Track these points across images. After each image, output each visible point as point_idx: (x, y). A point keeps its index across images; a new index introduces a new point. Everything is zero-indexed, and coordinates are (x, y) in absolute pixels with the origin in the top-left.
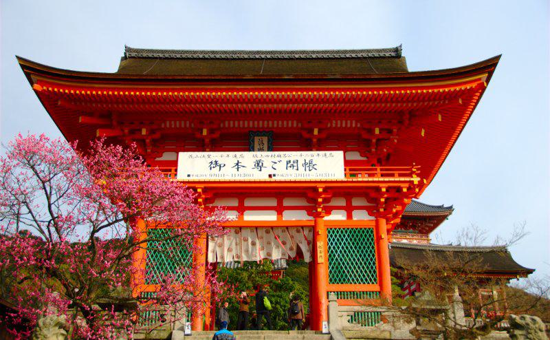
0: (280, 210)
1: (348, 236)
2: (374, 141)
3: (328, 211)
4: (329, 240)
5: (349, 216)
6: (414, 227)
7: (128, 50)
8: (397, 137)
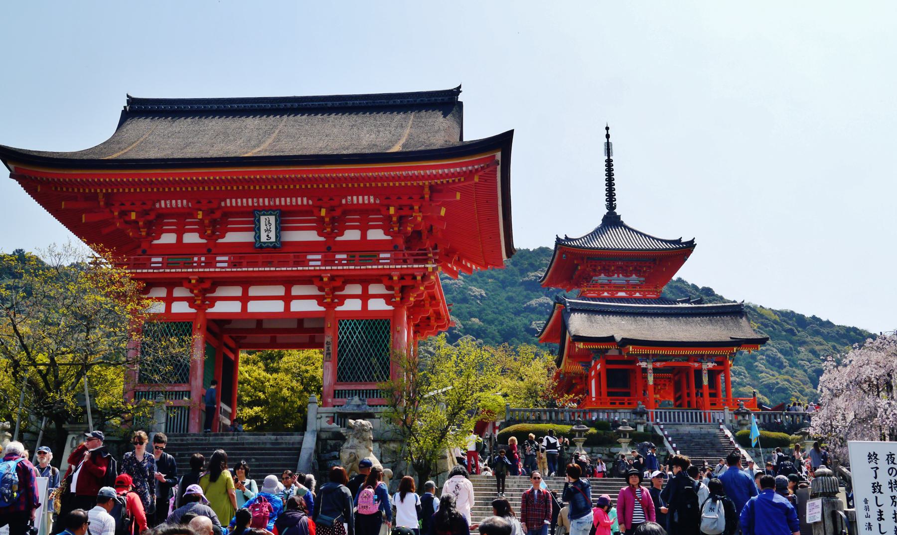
0: (287, 299)
1: (362, 328)
2: (394, 219)
3: (342, 299)
4: (341, 333)
5: (365, 305)
6: (638, 272)
7: (132, 101)
8: (421, 214)
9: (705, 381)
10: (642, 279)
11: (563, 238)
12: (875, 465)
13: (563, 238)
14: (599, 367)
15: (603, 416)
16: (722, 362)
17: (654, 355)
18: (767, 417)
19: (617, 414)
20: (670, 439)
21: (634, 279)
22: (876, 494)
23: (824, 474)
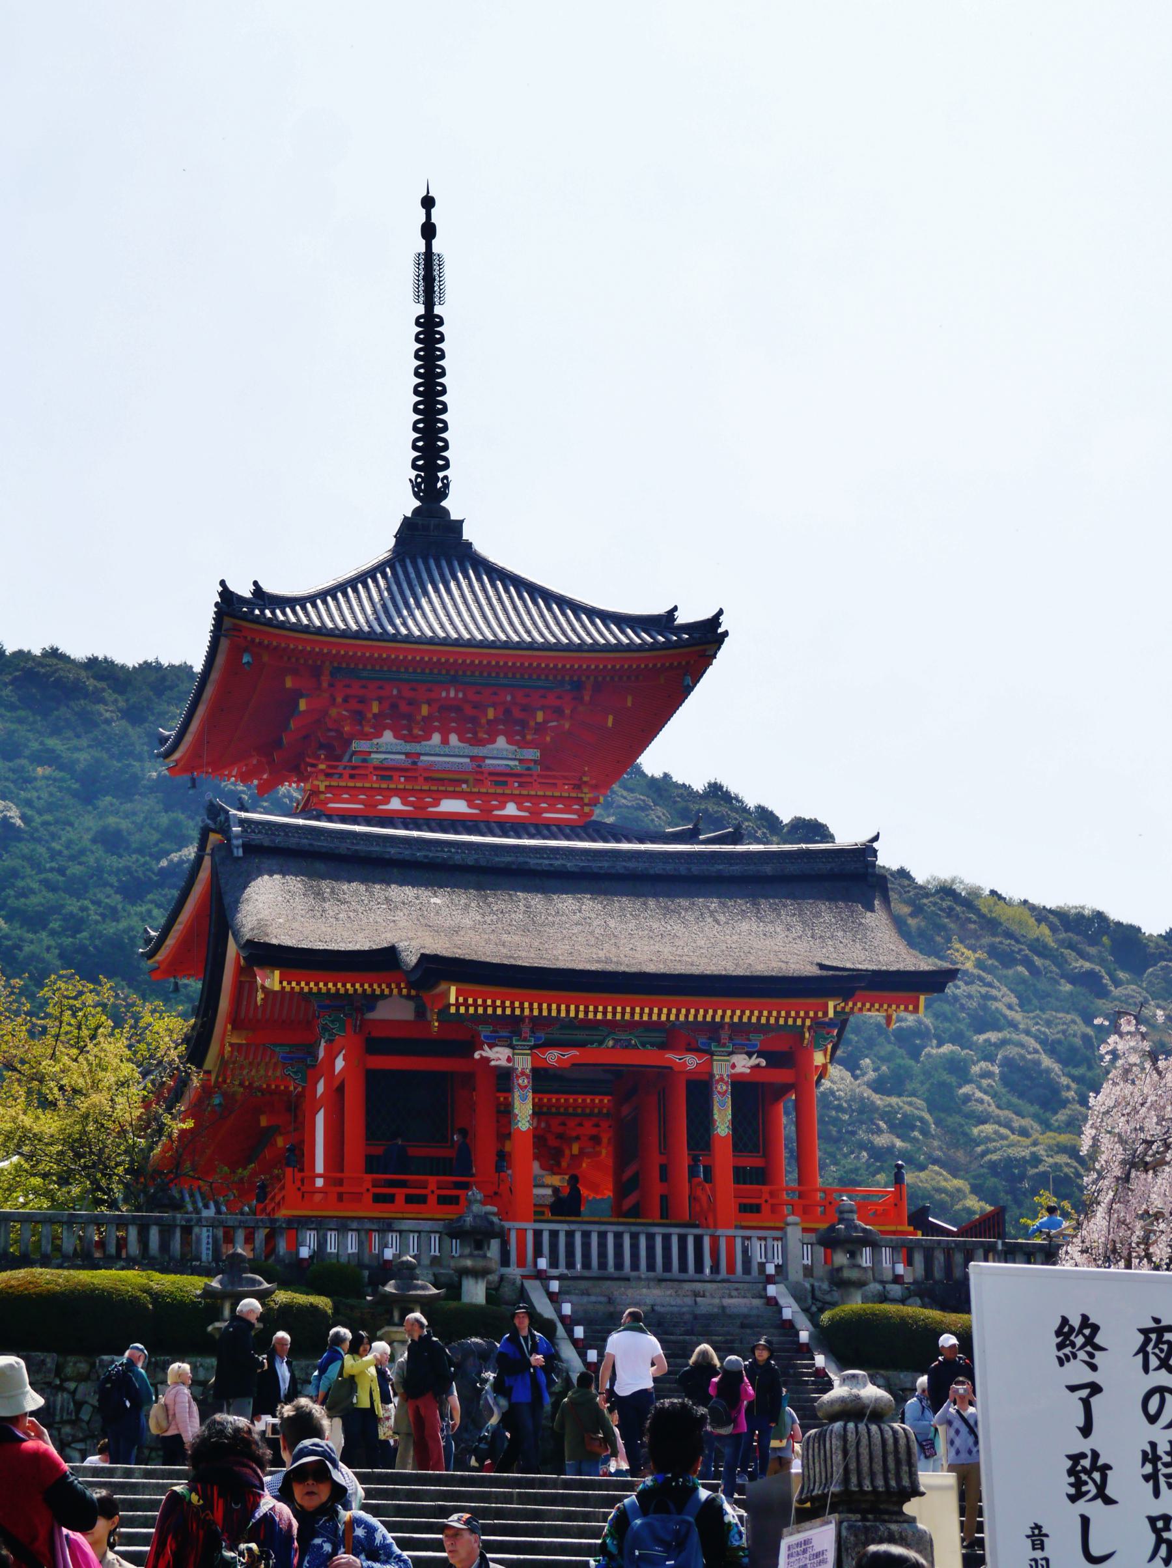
6: (515, 726)
9: (722, 1121)
10: (533, 754)
11: (246, 591)
12: (1088, 1376)
13: (246, 591)
14: (340, 1063)
15: (344, 1246)
16: (786, 1056)
17: (538, 1023)
18: (940, 1257)
19: (393, 1237)
20: (579, 1332)
21: (501, 752)
22: (1082, 1506)
23: (854, 1411)
